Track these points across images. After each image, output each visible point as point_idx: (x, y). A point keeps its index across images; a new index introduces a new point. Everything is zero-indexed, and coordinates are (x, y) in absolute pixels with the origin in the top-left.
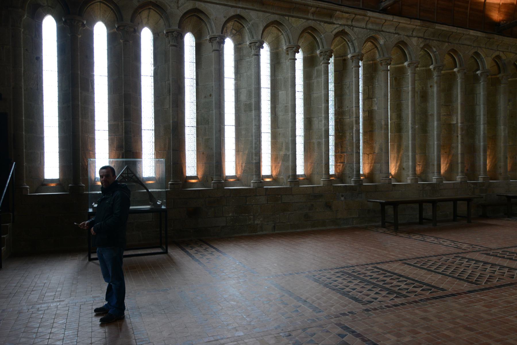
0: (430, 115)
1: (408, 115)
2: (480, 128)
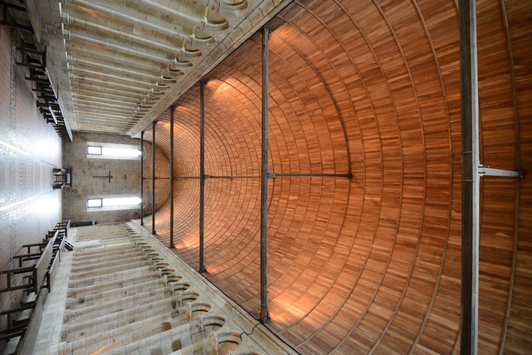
0: (146, 17)
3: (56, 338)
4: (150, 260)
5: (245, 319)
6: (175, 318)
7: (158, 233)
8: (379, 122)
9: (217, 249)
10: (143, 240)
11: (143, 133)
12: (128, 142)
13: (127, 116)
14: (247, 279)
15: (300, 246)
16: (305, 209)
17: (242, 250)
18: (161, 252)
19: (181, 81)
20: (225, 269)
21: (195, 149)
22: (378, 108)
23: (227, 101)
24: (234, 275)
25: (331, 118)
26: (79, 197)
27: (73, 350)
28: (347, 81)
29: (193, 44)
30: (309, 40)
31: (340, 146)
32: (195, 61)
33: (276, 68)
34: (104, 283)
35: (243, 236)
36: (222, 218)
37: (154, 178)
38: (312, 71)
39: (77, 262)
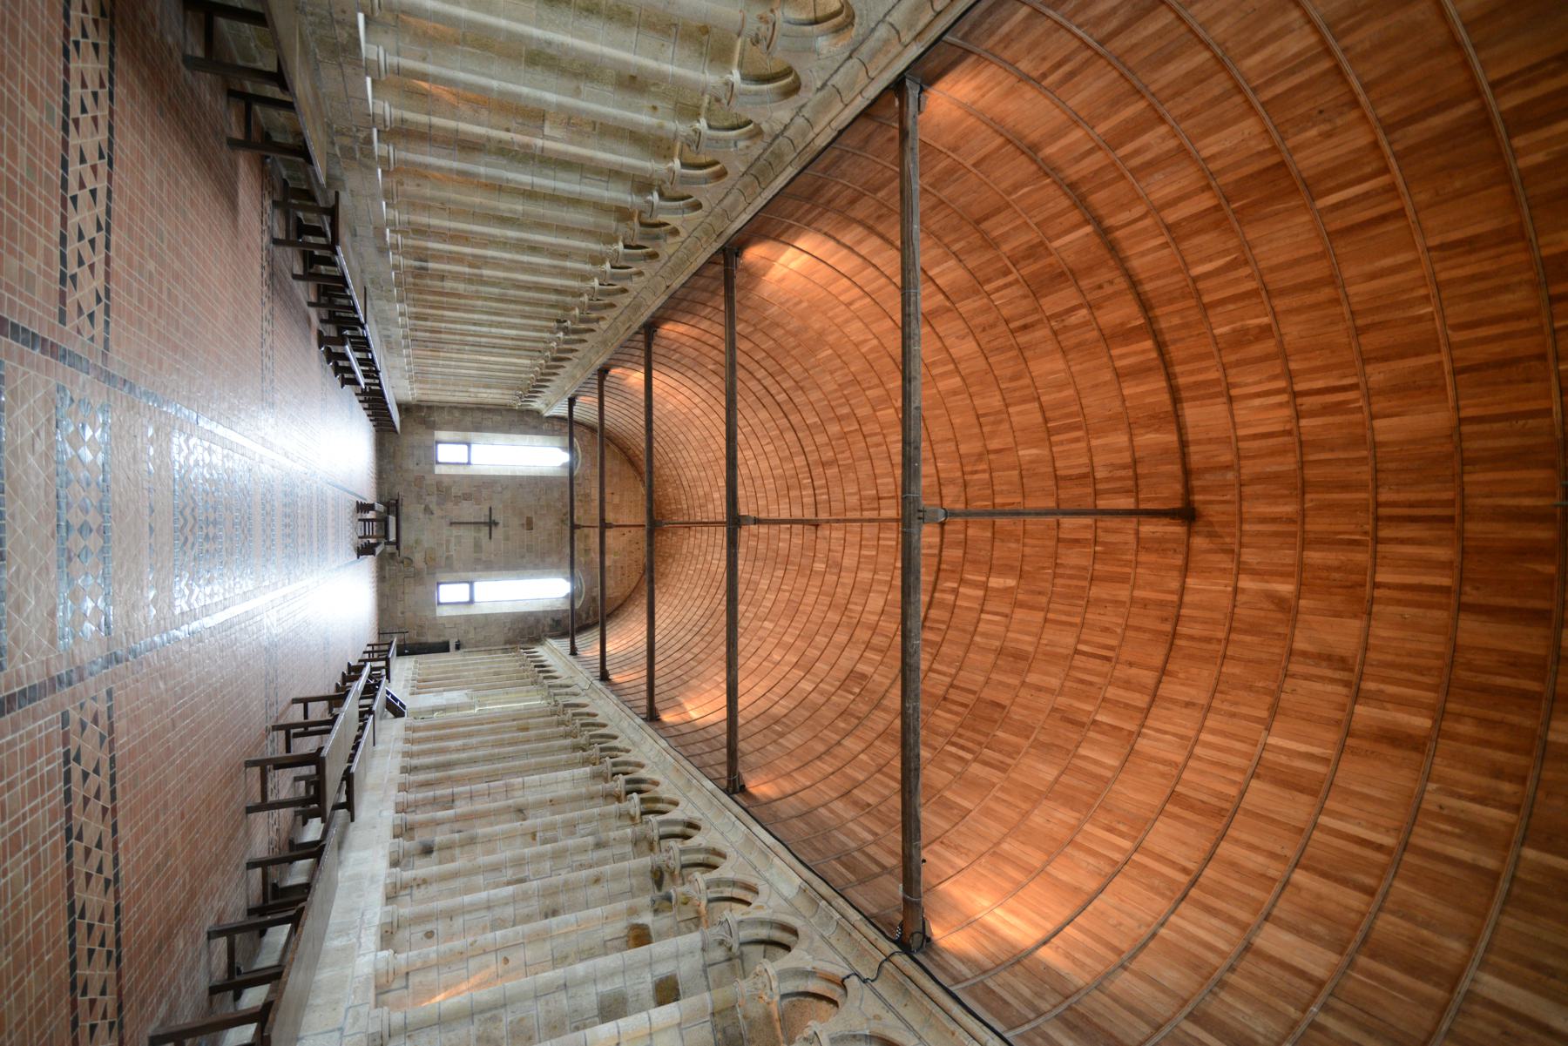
0: (578, 88)
1: (591, 37)
2: (524, 173)
3: (370, 939)
4: (594, 751)
5: (855, 935)
6: (661, 916)
7: (614, 678)
8: (1287, 339)
9: (777, 728)
10: (575, 695)
11: (572, 402)
12: (535, 427)
13: (531, 358)
14: (862, 819)
15: (1025, 730)
16: (1039, 616)
17: (848, 734)
18: (622, 731)
19: (671, 251)
20: (798, 788)
21: (711, 441)
22: (1282, 292)
23: (801, 302)
24: (824, 805)
25: (1125, 335)
26: (417, 577)
27: (407, 973)
28: (1172, 216)
29: (702, 147)
30: (1046, 97)
31: (1154, 420)
32: (707, 193)
33: (944, 194)
34: (481, 805)
35: (851, 693)
36: (788, 639)
37: (604, 526)
38: (1059, 193)
39: (415, 748)
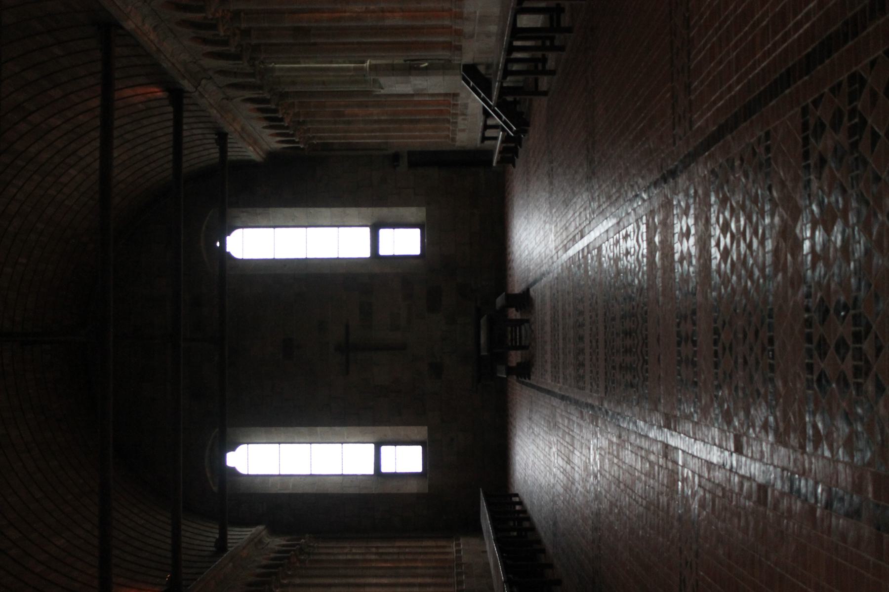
10: (223, 72)
